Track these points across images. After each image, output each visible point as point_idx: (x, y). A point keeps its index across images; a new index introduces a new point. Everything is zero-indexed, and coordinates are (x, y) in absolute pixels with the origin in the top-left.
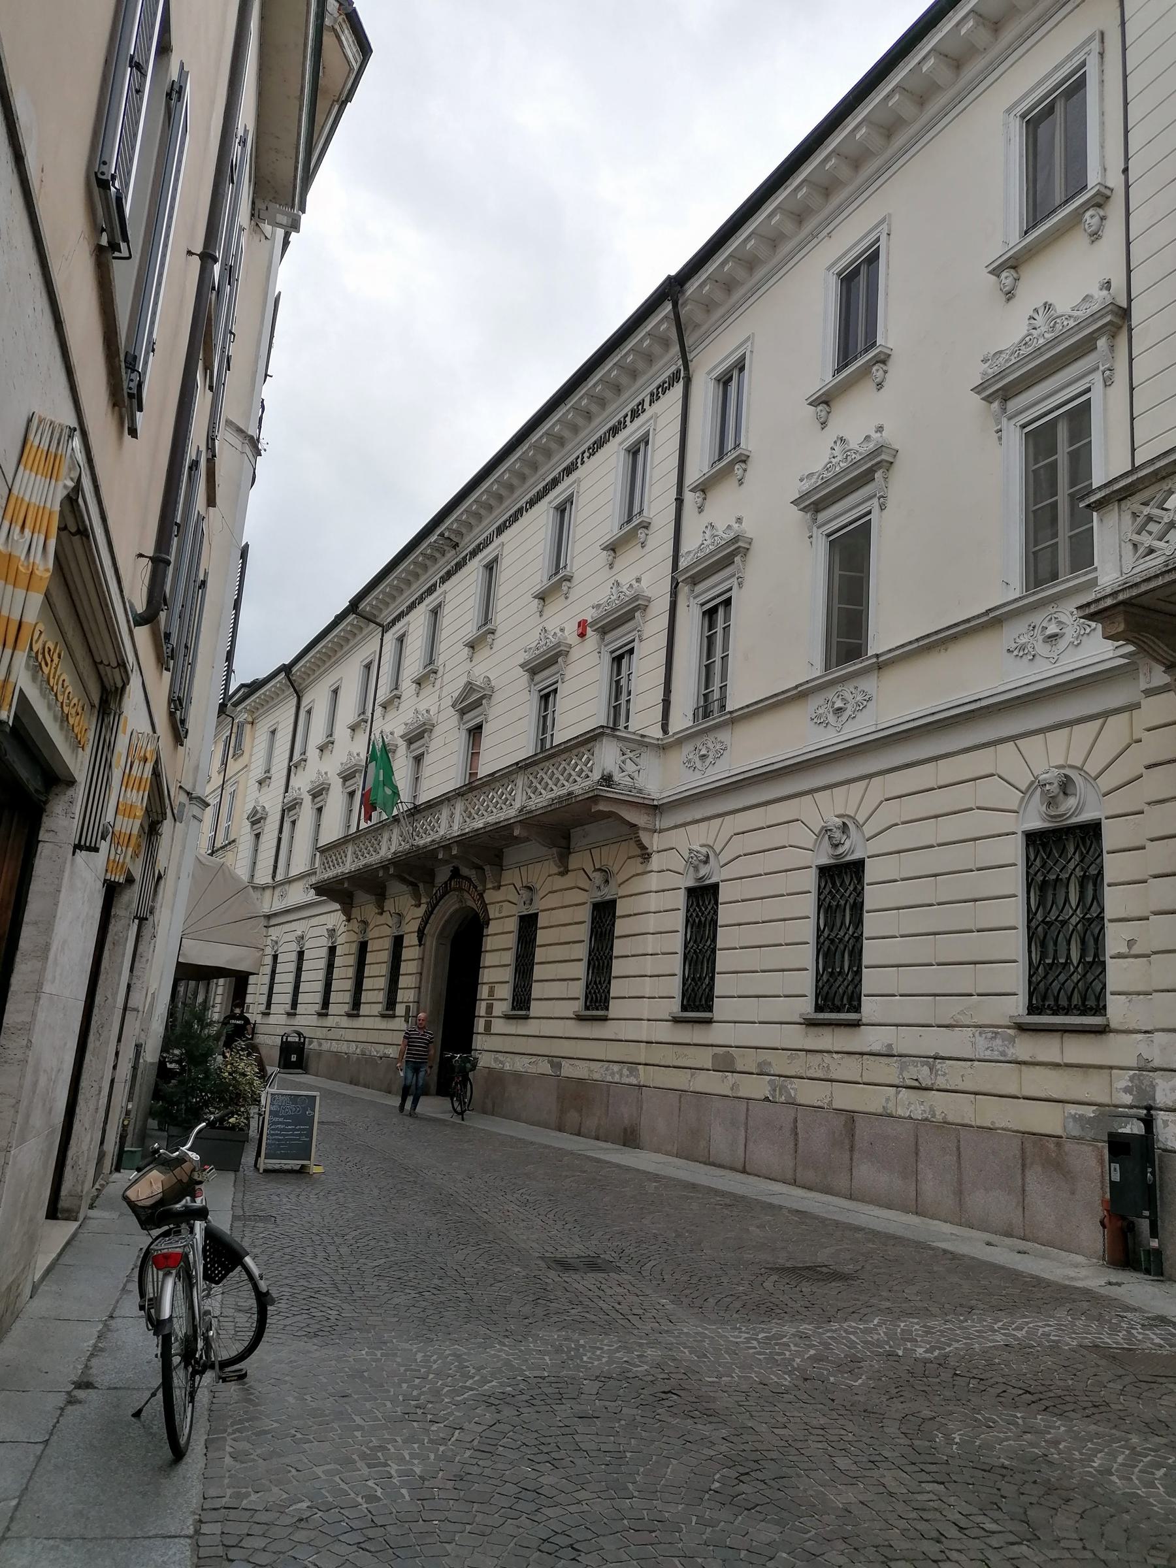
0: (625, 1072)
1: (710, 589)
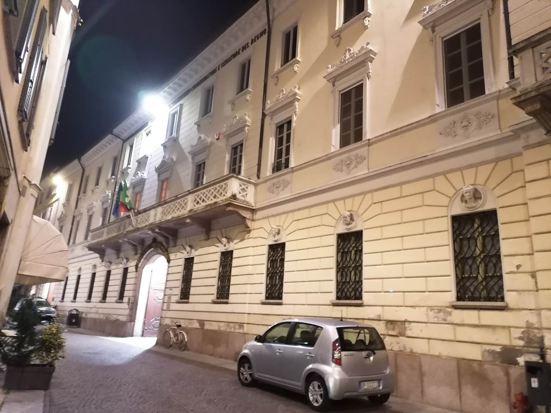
0: (237, 327)
1: (281, 118)
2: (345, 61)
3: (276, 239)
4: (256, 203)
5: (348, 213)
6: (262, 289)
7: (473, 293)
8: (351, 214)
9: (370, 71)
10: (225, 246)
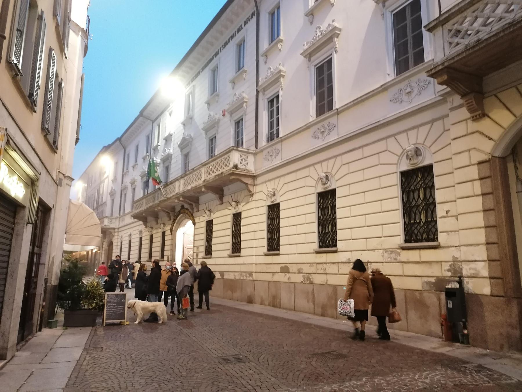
0: (248, 275)
1: (270, 93)
2: (316, 38)
3: (272, 200)
4: (256, 170)
5: (324, 174)
6: (265, 243)
7: (416, 236)
8: (327, 176)
9: (337, 46)
10: (235, 208)
